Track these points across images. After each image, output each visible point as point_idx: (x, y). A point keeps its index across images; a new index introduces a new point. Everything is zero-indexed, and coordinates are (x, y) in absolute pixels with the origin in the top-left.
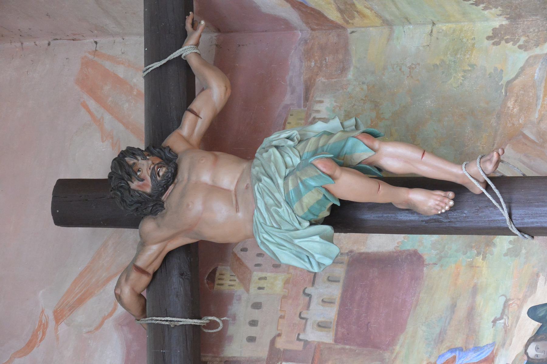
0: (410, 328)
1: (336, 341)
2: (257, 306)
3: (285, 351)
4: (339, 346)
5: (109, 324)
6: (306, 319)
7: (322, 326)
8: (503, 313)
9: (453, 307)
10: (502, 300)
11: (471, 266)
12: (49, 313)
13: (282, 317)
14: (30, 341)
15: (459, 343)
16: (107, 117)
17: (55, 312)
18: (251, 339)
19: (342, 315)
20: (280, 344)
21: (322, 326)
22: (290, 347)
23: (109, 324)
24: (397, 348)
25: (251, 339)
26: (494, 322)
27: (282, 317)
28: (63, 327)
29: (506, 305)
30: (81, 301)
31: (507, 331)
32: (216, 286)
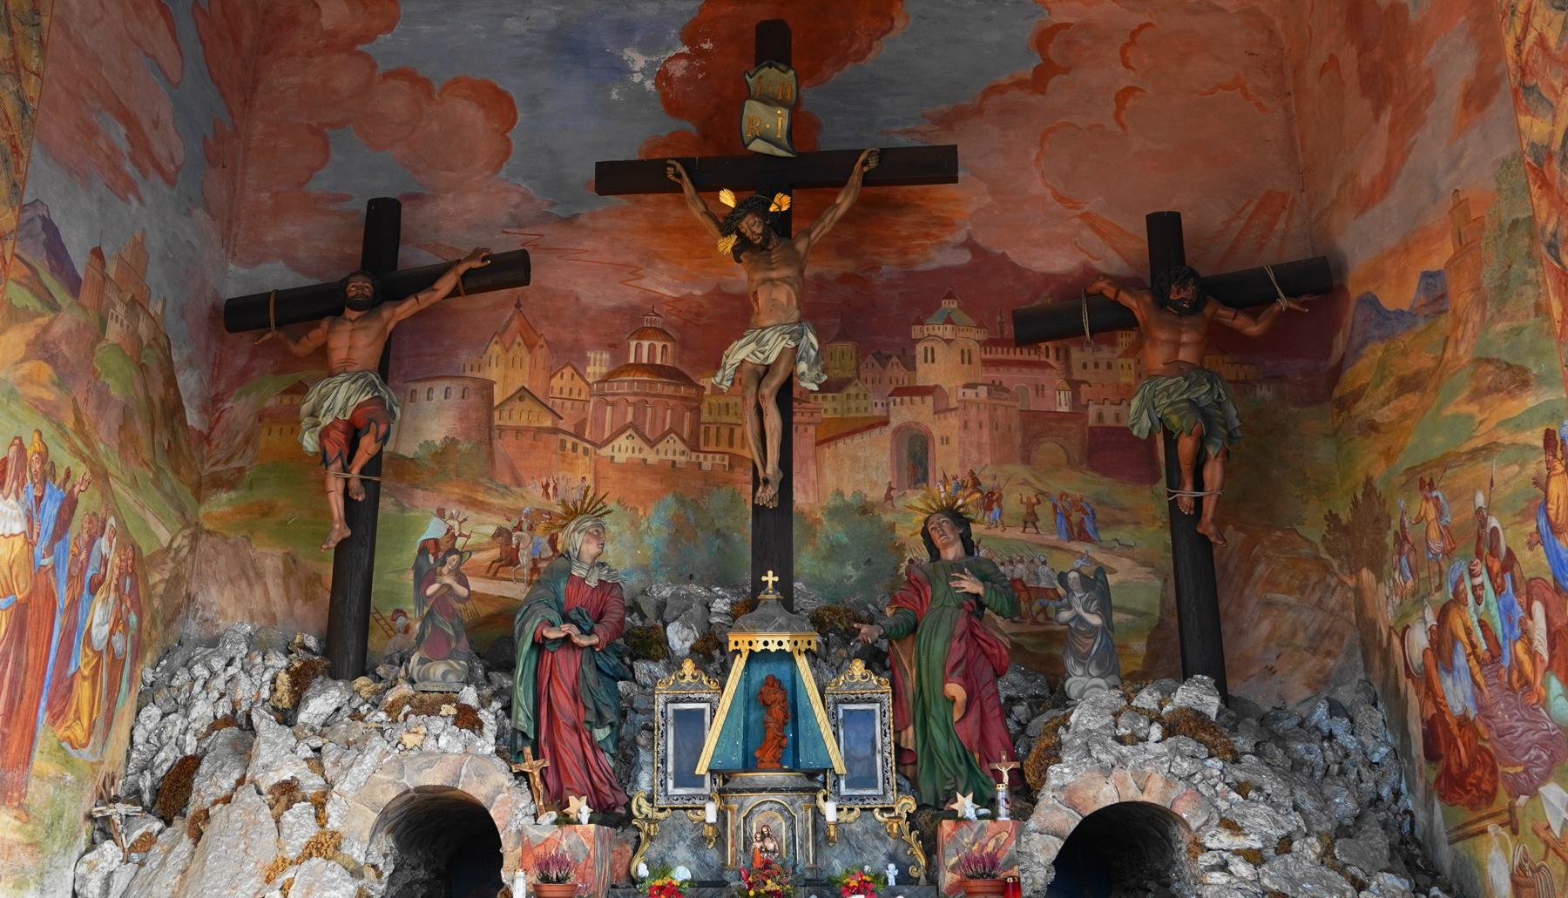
0: (1105, 480)
1: (1090, 428)
2: (1109, 366)
3: (1079, 393)
4: (1087, 430)
5: (1084, 257)
6: (1103, 404)
7: (1100, 416)
8: (1123, 545)
9: (1123, 509)
10: (1132, 544)
11: (1154, 519)
12: (1086, 209)
13: (1103, 386)
14: (1063, 198)
15: (1098, 516)
16: (1242, 222)
17: (1088, 213)
18: (1085, 366)
19: (1110, 430)
20: (1084, 388)
21: (1100, 416)
22: (1082, 395)
23: (1084, 257)
24: (1090, 473)
25: (1085, 366)
26: (1116, 540)
27: (1103, 386)
28: (1077, 221)
29: (1129, 546)
30: (1098, 231)
31: (1110, 550)
32: (1120, 333)
